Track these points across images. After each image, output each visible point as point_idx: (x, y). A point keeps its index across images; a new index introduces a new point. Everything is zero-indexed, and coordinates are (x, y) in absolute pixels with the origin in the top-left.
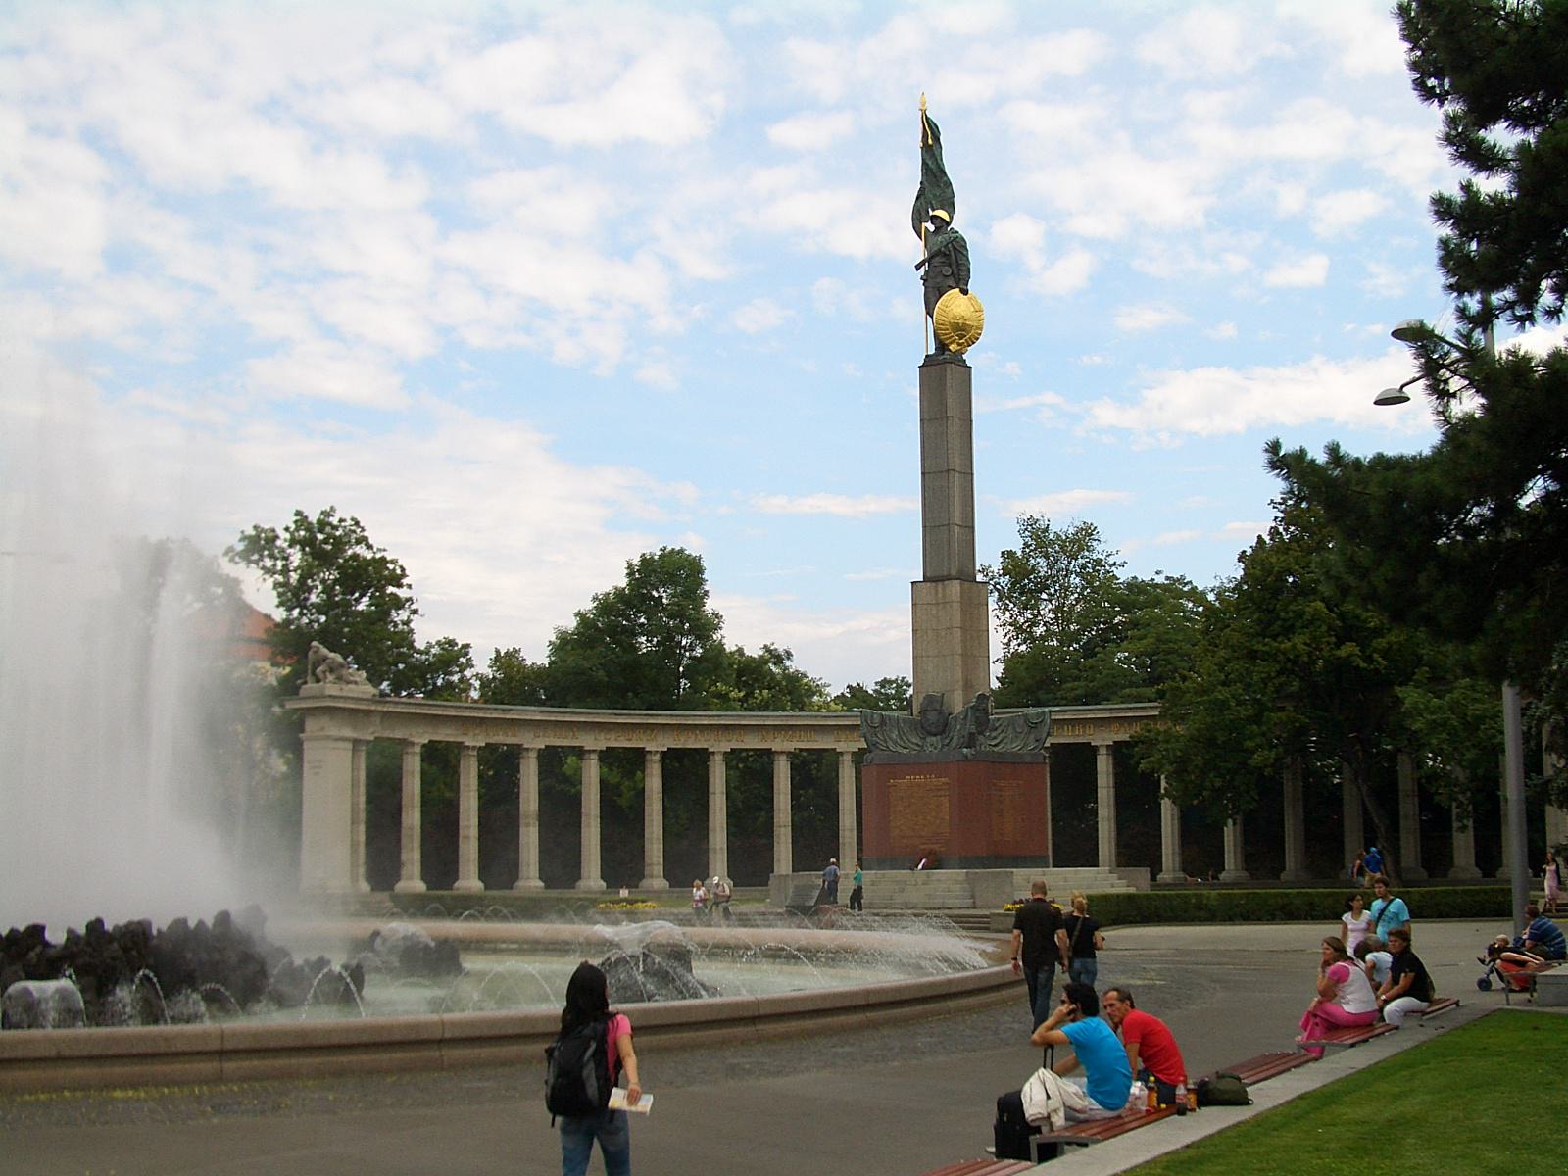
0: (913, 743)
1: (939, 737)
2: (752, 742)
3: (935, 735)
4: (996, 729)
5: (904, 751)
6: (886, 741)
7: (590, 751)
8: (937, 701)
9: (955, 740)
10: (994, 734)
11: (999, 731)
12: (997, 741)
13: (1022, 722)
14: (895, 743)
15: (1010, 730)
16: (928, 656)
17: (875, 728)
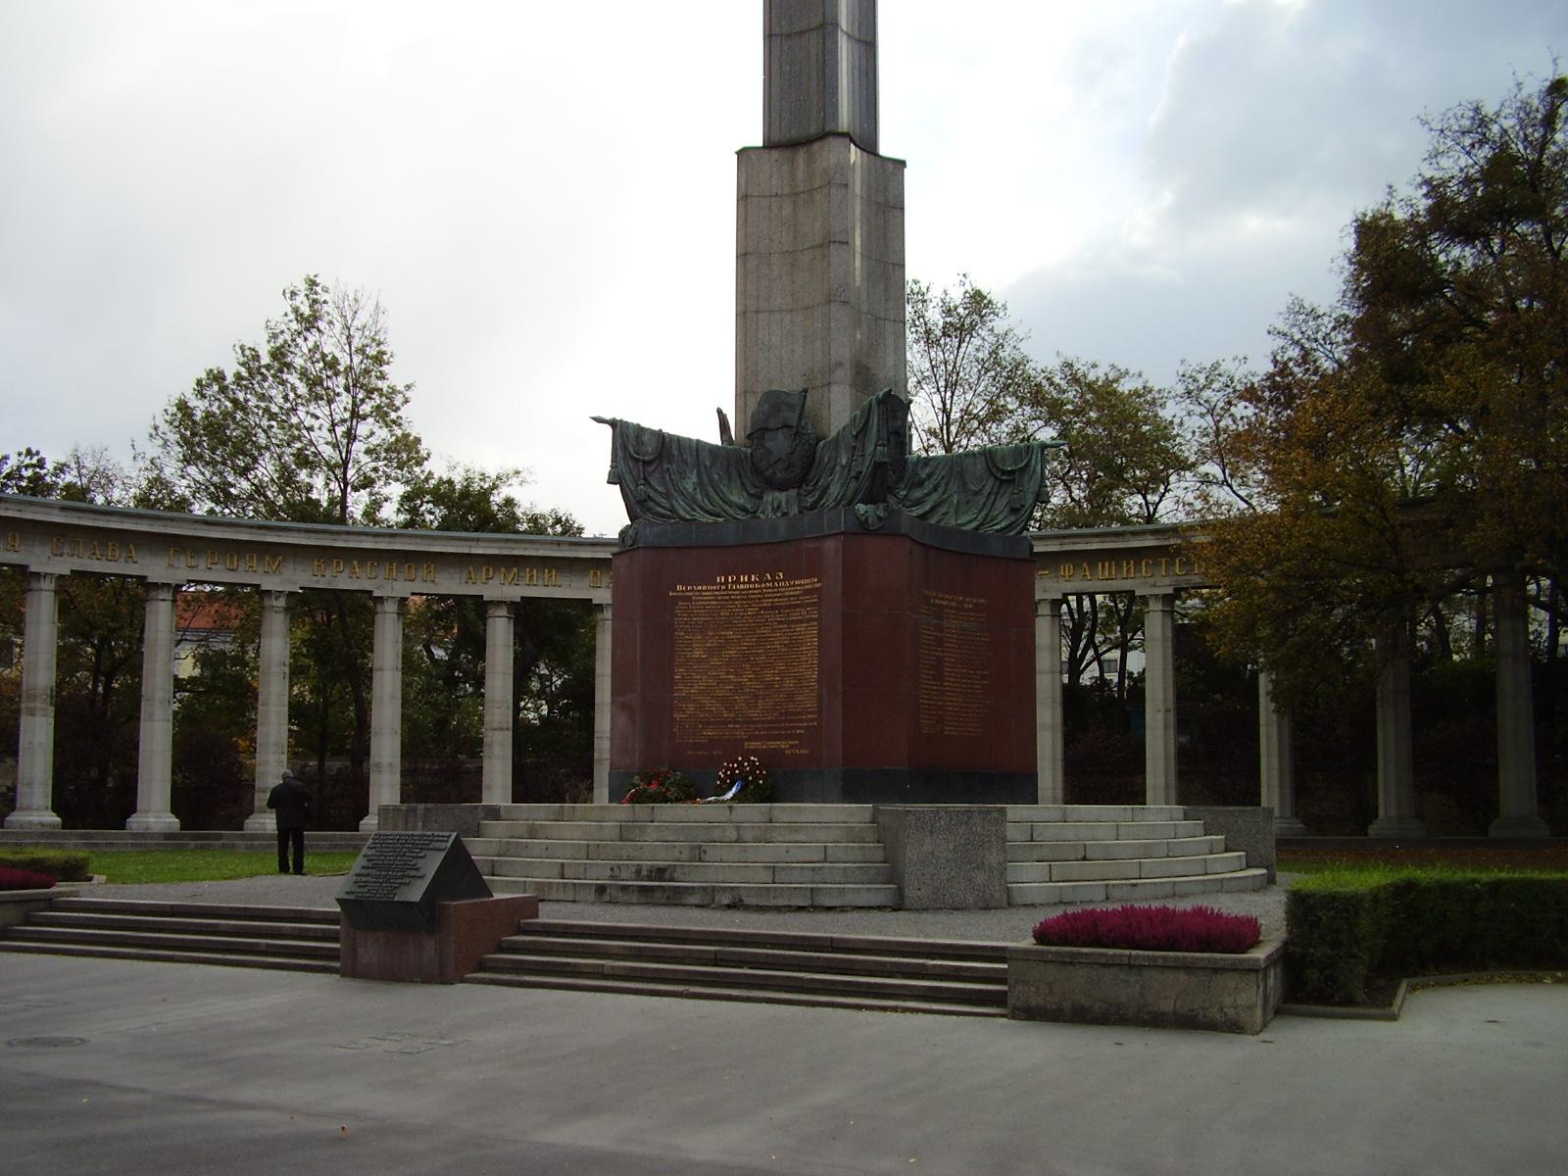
0: (731, 504)
1: (793, 493)
2: (451, 584)
3: (782, 488)
4: (921, 484)
5: (711, 519)
6: (667, 496)
7: (157, 586)
8: (791, 407)
9: (834, 490)
10: (918, 494)
11: (928, 486)
12: (927, 507)
13: (980, 466)
14: (691, 501)
15: (953, 487)
16: (771, 312)
17: (646, 463)
